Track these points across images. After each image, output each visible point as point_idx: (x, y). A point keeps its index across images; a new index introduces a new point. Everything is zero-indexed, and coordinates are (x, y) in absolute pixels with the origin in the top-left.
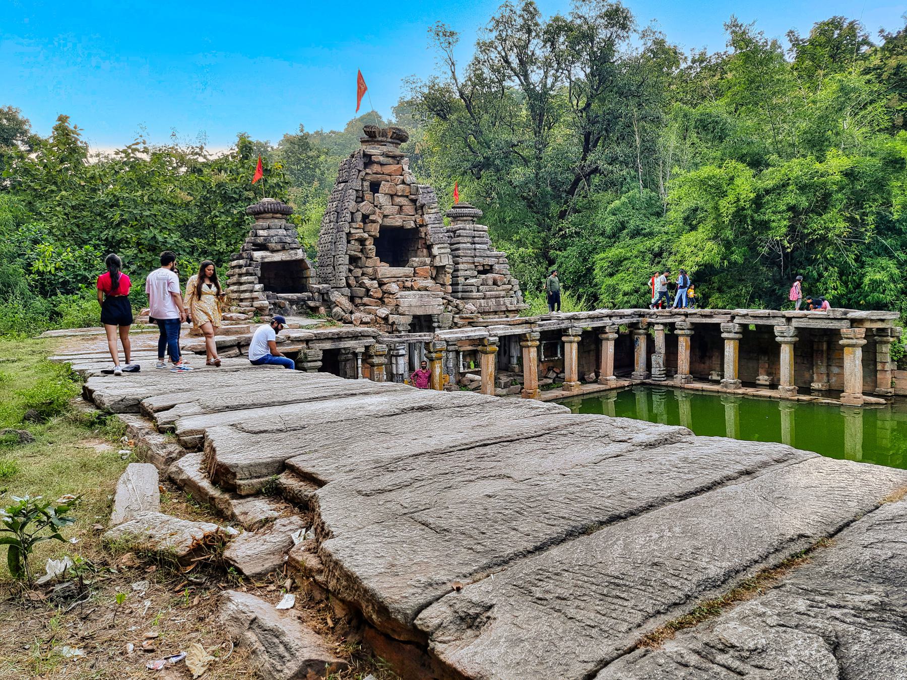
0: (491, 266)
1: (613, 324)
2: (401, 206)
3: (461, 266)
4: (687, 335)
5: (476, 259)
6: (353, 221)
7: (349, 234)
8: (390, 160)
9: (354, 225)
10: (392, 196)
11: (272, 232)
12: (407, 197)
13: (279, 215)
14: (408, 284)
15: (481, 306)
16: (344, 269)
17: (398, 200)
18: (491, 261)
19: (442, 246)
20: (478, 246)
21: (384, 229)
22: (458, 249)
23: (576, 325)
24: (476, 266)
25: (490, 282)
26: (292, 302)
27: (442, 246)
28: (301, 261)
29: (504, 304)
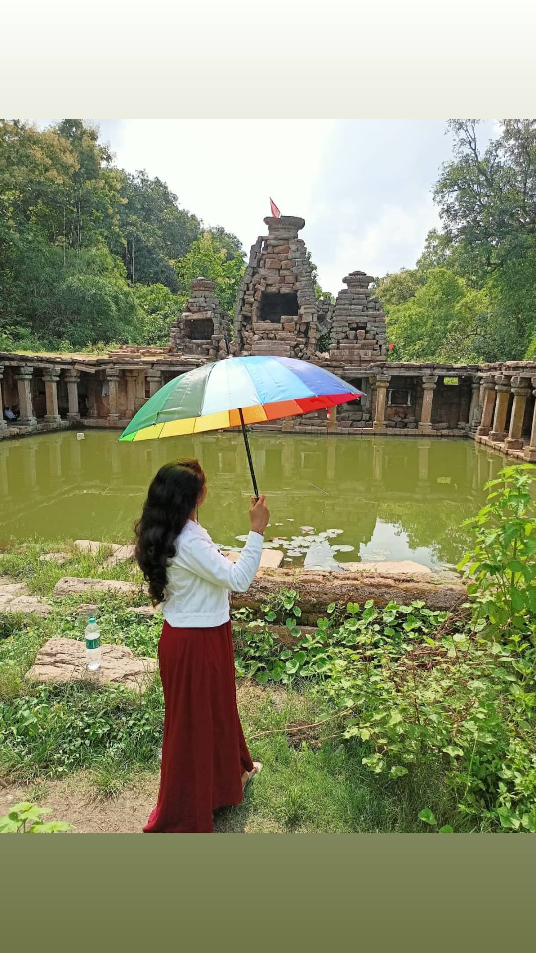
1: (432, 375)
3: (334, 324)
4: (431, 389)
5: (349, 318)
6: (248, 289)
8: (281, 242)
11: (196, 300)
14: (272, 335)
15: (333, 354)
17: (282, 272)
18: (364, 319)
20: (353, 307)
21: (265, 295)
25: (351, 336)
26: (198, 346)
28: (210, 320)
29: (358, 354)
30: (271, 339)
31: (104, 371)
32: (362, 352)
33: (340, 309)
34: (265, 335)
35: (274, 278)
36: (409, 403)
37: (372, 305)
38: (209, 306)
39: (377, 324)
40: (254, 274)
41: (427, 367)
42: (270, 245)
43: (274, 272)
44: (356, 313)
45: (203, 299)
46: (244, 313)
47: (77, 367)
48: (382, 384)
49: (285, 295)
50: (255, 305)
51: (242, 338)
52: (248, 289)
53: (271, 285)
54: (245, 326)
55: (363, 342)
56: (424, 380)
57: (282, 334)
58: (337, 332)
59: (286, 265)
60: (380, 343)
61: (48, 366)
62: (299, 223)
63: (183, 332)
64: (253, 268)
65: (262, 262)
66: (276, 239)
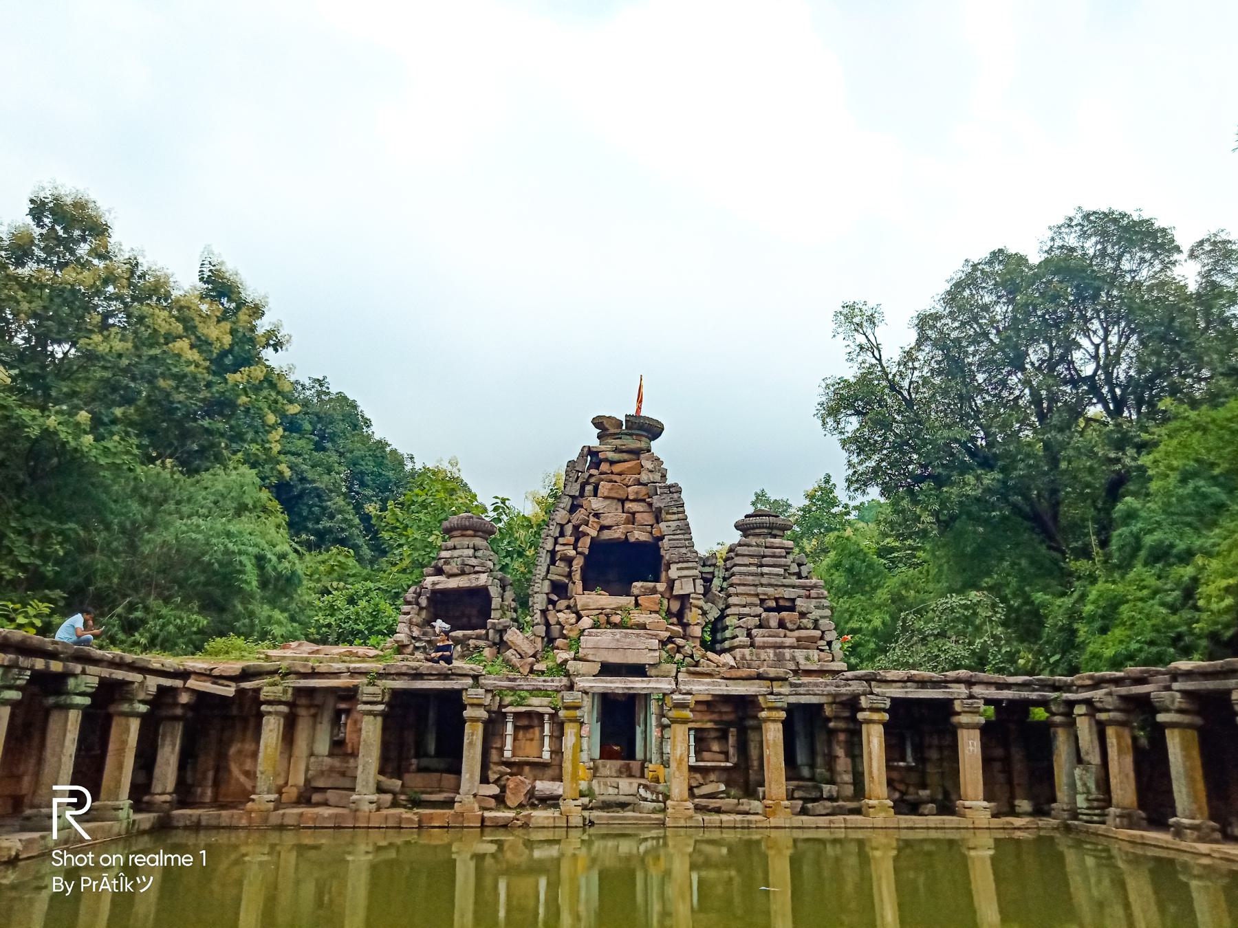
0: (793, 600)
2: (633, 514)
3: (732, 600)
5: (760, 590)
6: (562, 534)
7: (553, 553)
8: (625, 456)
9: (561, 540)
10: (623, 501)
11: (456, 553)
12: (644, 500)
13: (470, 532)
15: (743, 658)
16: (539, 602)
17: (628, 505)
18: (789, 593)
19: (685, 565)
20: (765, 570)
22: (733, 575)
23: (876, 690)
24: (762, 601)
25: (774, 623)
27: (685, 565)
29: (793, 658)
30: (615, 626)
31: (257, 691)
32: (800, 654)
33: (741, 574)
34: (603, 618)
35: (612, 515)
36: (910, 759)
37: (794, 568)
38: (482, 565)
40: (573, 509)
41: (958, 681)
42: (606, 460)
43: (617, 505)
44: (773, 581)
45: (471, 552)
46: (555, 577)
47: (192, 683)
48: (876, 716)
49: (639, 544)
50: (578, 563)
51: (548, 625)
52: (562, 534)
53: (609, 528)
54: (553, 603)
55: (796, 633)
56: (958, 706)
57: (638, 617)
58: (741, 617)
59: (637, 493)
60: (828, 637)
62: (653, 430)
63: (424, 614)
64: (573, 497)
65: (589, 488)
66: (616, 450)
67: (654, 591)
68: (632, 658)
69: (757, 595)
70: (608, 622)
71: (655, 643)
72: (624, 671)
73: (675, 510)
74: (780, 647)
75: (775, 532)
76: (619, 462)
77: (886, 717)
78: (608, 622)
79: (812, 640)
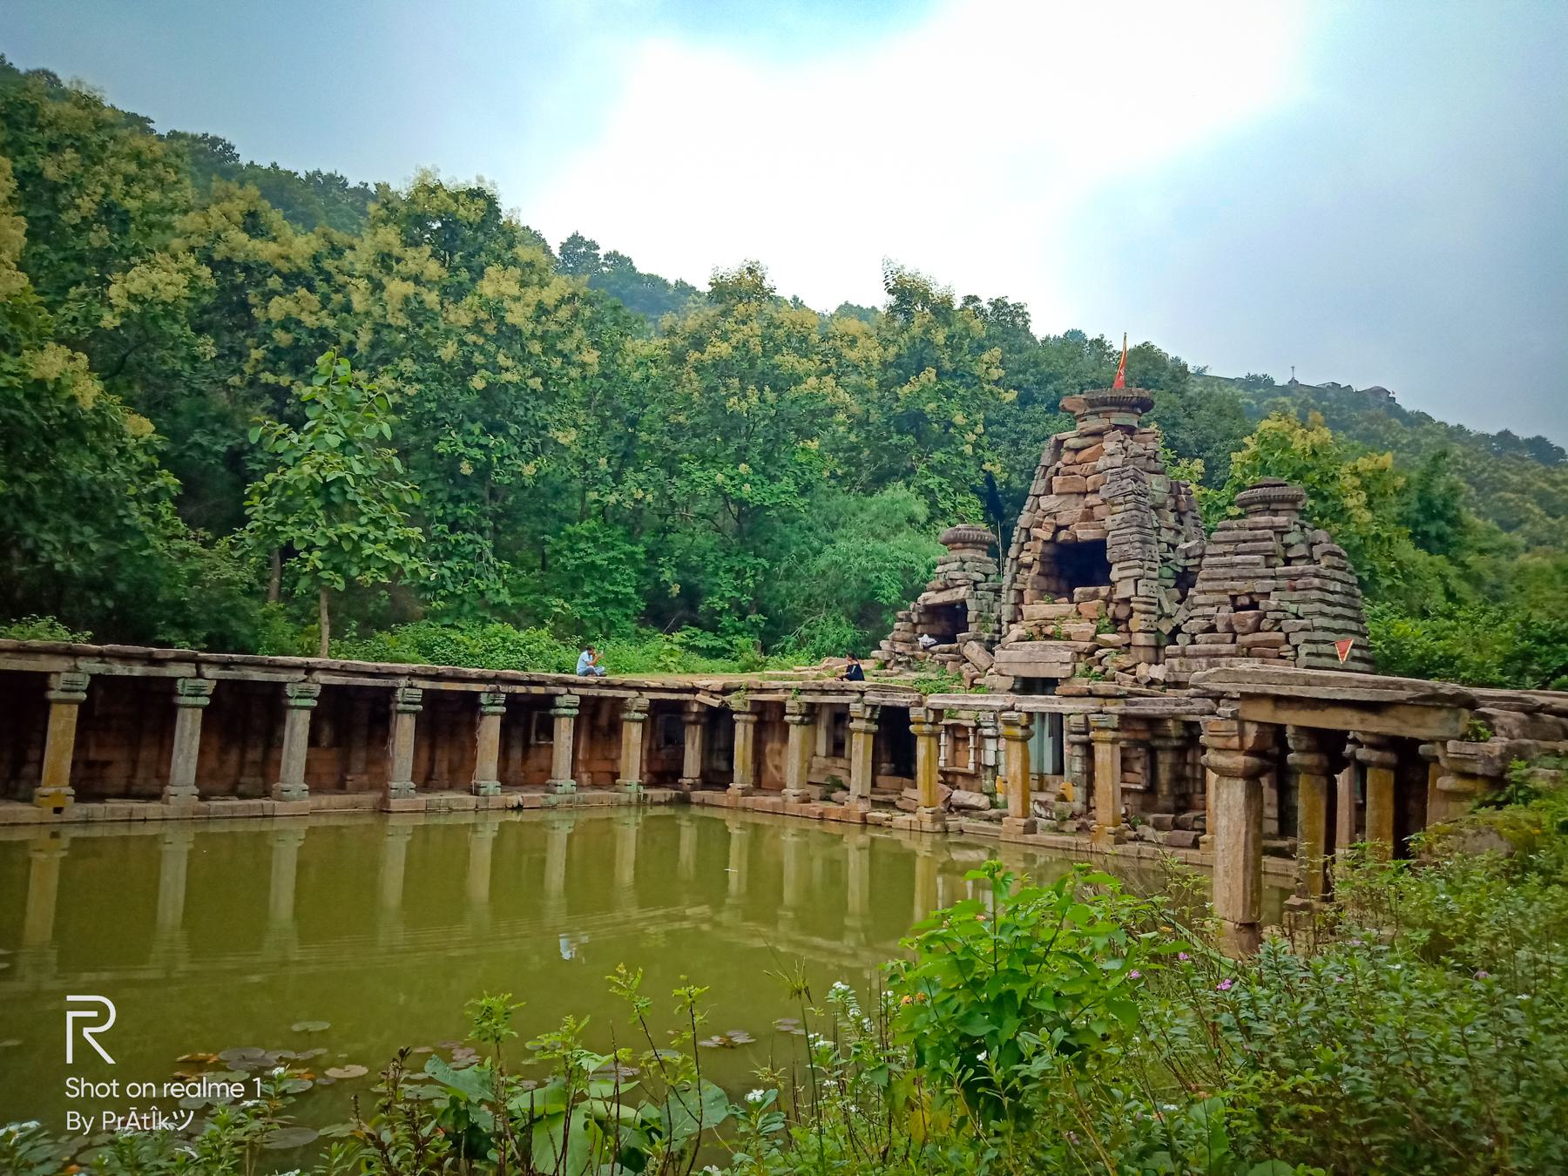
5: (1228, 584)
8: (1090, 440)
30: (1048, 637)
33: (1211, 566)
39: (1296, 596)
44: (1245, 573)
55: (1249, 638)
61: (621, 694)
67: (1095, 596)
68: (1043, 672)
69: (1225, 591)
70: (1041, 633)
71: (1067, 655)
72: (1038, 687)
73: (1121, 499)
74: (1216, 656)
75: (1273, 506)
76: (1083, 448)
77: (576, 712)
78: (1041, 633)
79: (1274, 644)
